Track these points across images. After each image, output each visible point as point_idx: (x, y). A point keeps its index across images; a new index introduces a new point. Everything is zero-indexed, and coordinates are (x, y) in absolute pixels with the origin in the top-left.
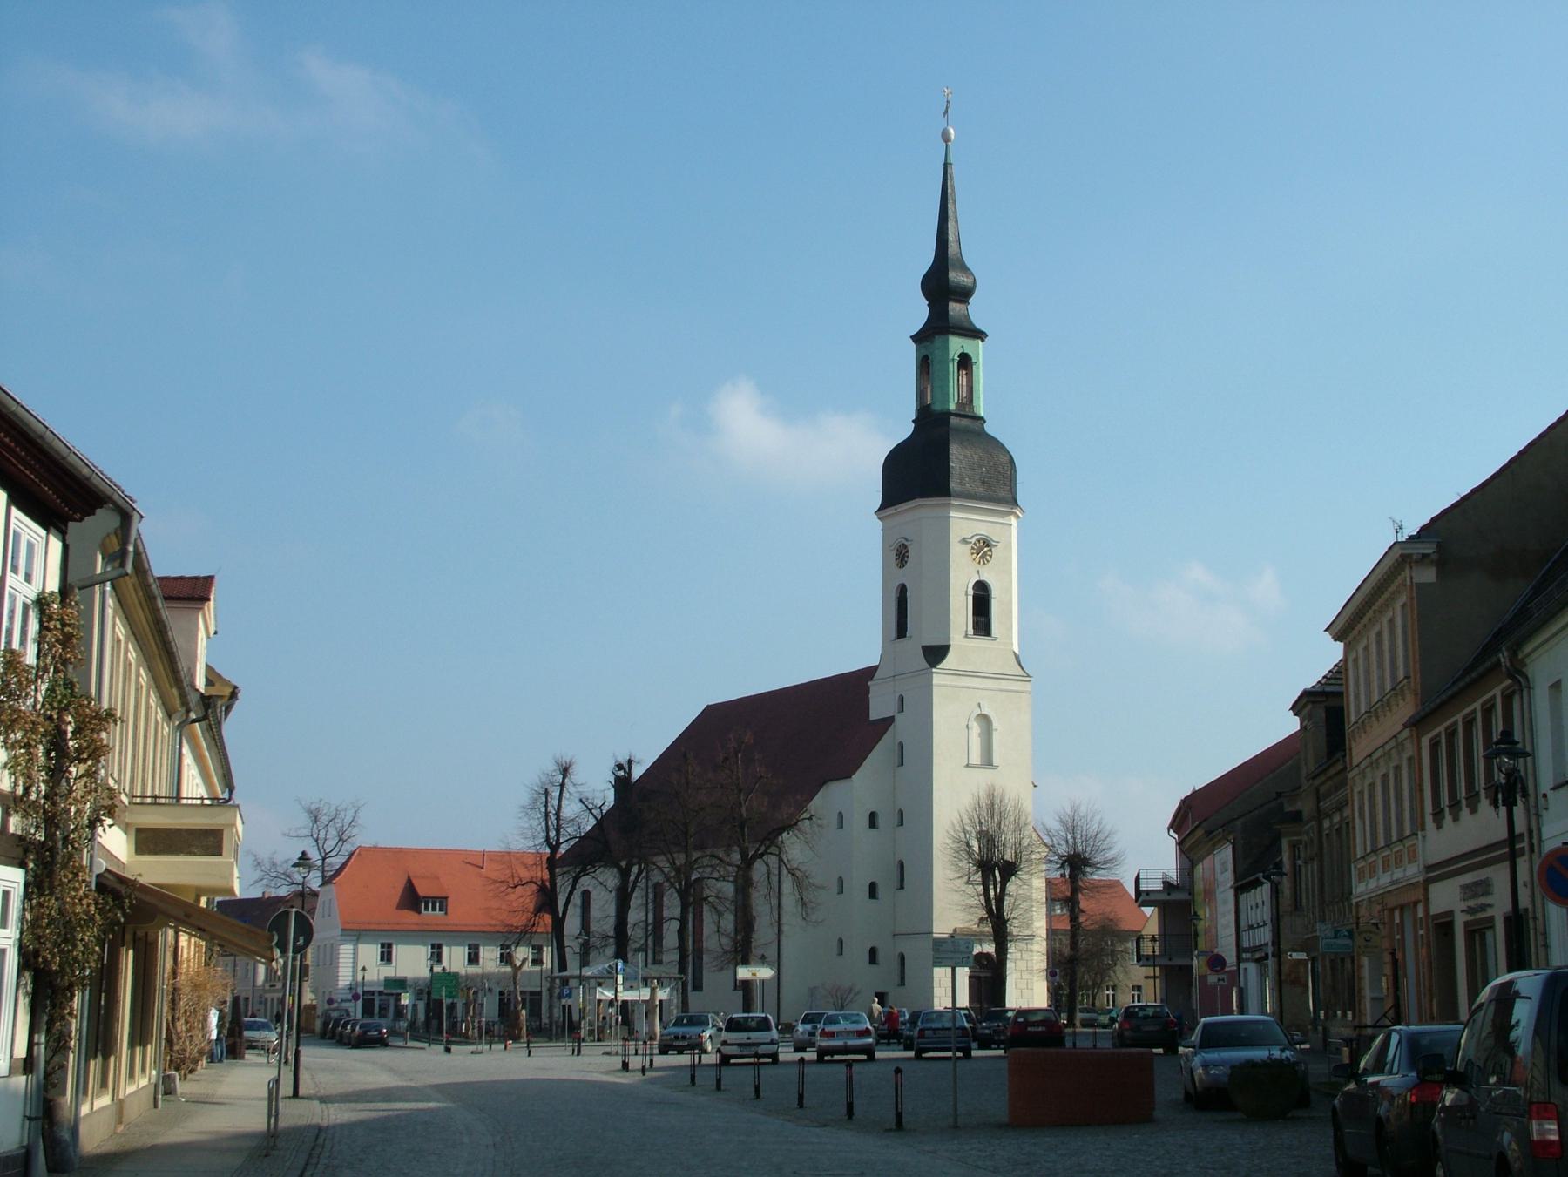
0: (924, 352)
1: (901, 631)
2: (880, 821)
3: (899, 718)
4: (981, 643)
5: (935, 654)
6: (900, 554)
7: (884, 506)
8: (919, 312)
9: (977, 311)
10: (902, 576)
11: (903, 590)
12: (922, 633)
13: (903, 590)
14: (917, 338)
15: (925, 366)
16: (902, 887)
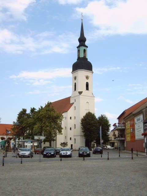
0: (78, 49)
1: (75, 90)
2: (72, 118)
3: (75, 103)
4: (87, 91)
5: (80, 93)
6: (75, 78)
7: (72, 72)
8: (78, 44)
9: (87, 43)
10: (75, 81)
11: (75, 83)
12: (79, 89)
13: (75, 83)
14: (78, 47)
15: (79, 51)
16: (75, 128)
